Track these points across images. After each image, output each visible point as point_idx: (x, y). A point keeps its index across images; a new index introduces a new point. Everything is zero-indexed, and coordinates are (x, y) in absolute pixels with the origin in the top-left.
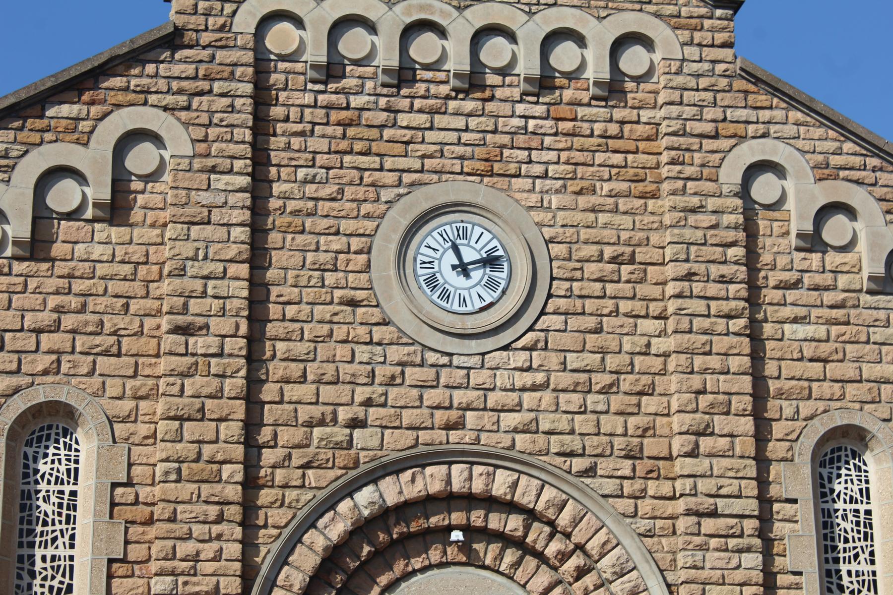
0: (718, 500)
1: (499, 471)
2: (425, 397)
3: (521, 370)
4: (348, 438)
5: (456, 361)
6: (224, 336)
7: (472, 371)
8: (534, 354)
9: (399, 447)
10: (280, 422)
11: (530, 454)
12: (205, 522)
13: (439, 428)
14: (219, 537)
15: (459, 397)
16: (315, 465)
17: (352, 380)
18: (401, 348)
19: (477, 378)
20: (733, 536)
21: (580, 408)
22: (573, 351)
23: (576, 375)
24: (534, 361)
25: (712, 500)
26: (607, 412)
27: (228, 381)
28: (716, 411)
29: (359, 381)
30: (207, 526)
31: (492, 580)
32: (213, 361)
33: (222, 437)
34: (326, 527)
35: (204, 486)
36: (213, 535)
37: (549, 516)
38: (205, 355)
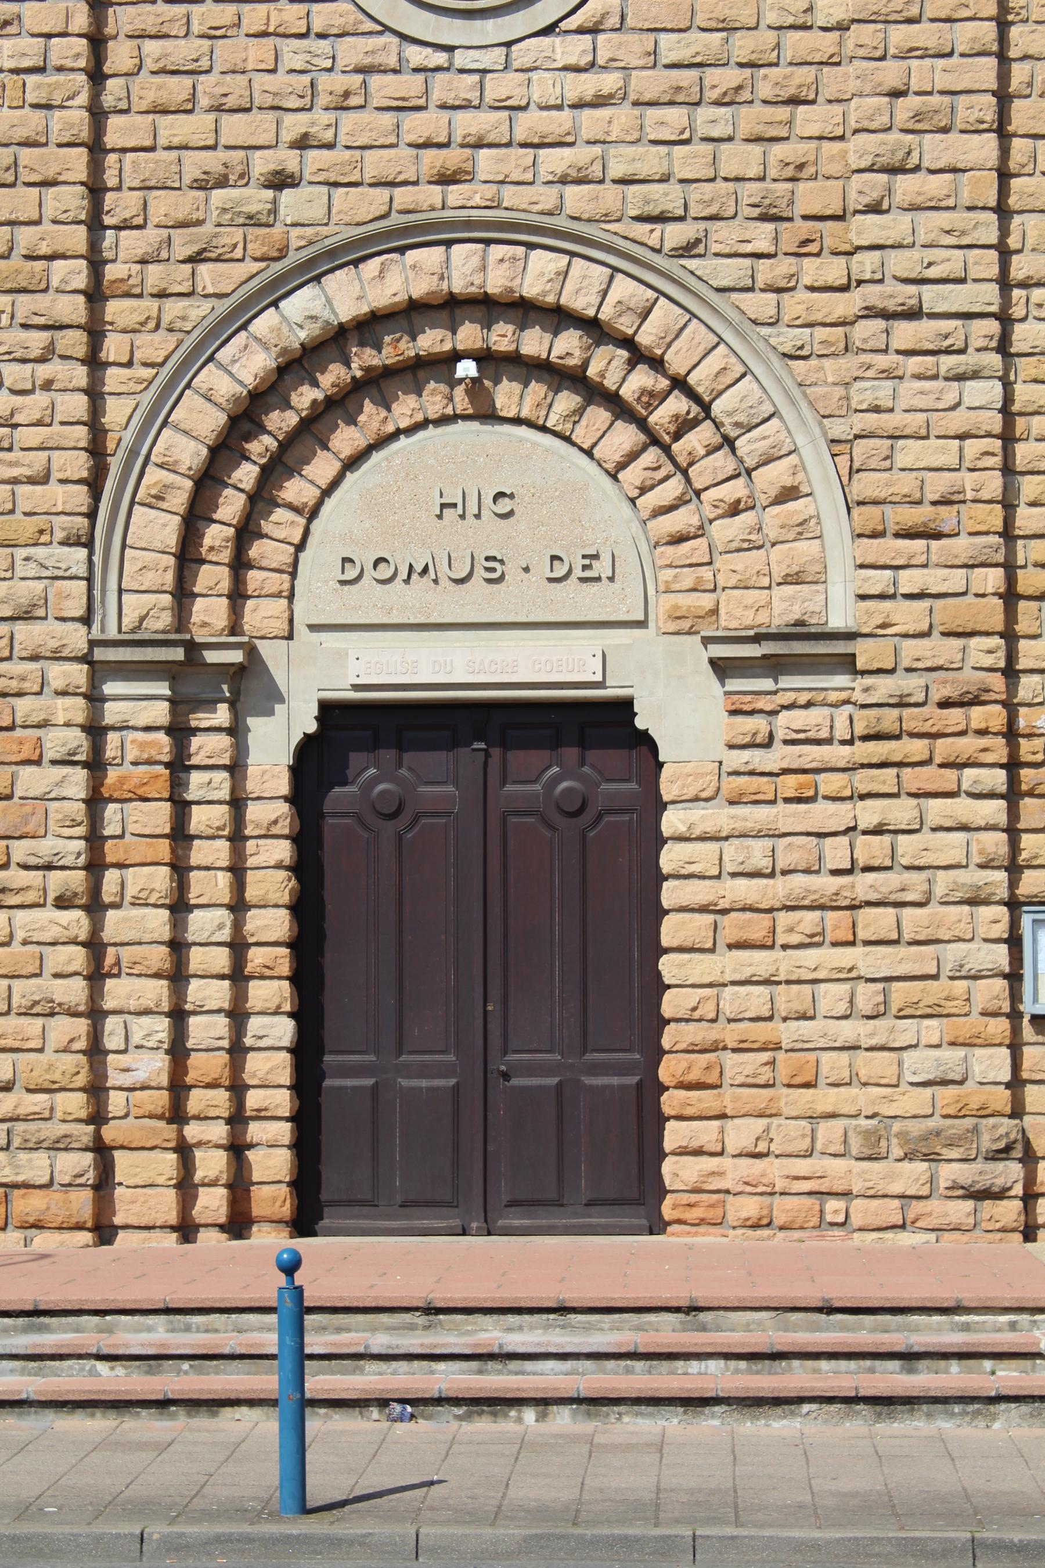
0: (925, 288)
1: (536, 254)
2: (405, 127)
3: (577, 69)
4: (269, 206)
5: (461, 59)
6: (49, 36)
7: (489, 76)
8: (601, 38)
9: (358, 219)
10: (152, 183)
11: (589, 220)
12: (24, 361)
13: (430, 183)
14: (48, 385)
15: (467, 123)
16: (213, 255)
17: (276, 102)
18: (361, 40)
19: (498, 87)
20: (948, 352)
21: (682, 133)
22: (672, 30)
23: (675, 73)
24: (599, 53)
25: (912, 289)
26: (730, 139)
27: (57, 114)
28: (927, 127)
29: (290, 105)
30: (29, 366)
31: (533, 444)
32: (31, 79)
33: (49, 213)
34: (234, 362)
35: (22, 298)
36: (38, 383)
37: (623, 328)
38: (12, 71)
